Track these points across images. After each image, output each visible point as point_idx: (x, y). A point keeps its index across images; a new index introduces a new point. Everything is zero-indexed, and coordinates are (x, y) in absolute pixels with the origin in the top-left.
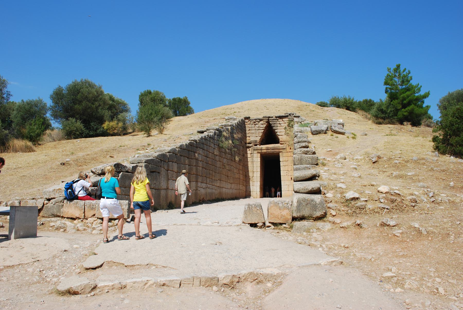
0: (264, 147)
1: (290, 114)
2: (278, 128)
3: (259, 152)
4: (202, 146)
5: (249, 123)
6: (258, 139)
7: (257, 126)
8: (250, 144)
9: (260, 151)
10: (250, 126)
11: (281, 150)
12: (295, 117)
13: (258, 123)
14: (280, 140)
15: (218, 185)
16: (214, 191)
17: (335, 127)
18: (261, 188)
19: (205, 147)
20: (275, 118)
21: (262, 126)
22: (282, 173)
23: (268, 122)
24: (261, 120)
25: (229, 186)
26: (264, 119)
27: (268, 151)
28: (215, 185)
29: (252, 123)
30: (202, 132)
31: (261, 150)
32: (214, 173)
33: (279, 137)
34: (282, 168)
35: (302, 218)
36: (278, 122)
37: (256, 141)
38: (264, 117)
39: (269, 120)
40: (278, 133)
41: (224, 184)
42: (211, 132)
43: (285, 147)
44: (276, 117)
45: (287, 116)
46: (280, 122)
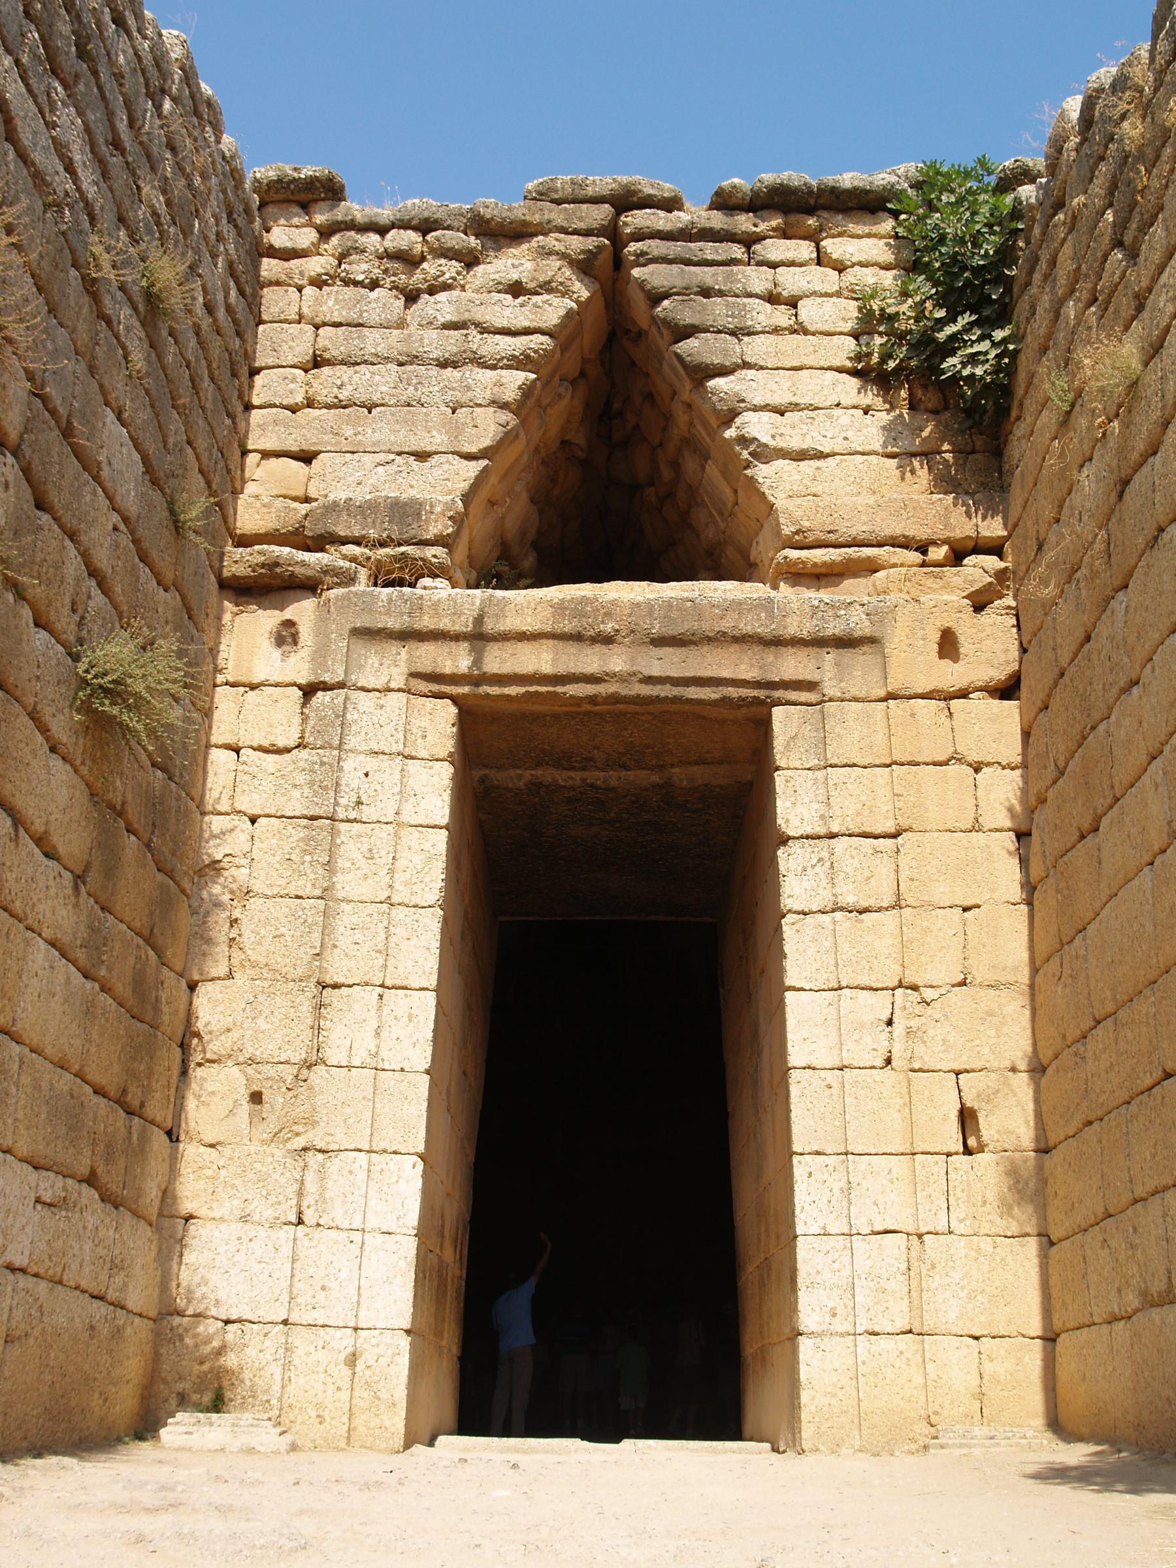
0: (529, 605)
2: (756, 348)
5: (316, 265)
6: (443, 486)
9: (458, 660)
10: (333, 303)
11: (792, 665)
13: (450, 268)
18: (428, 1273)
20: (717, 220)
21: (510, 312)
23: (607, 266)
24: (503, 234)
26: (556, 215)
27: (590, 660)
29: (359, 269)
31: (478, 637)
33: (763, 473)
34: (806, 953)
36: (758, 279)
37: (405, 511)
39: (612, 231)
40: (757, 426)
43: (857, 622)
44: (724, 202)
46: (791, 281)
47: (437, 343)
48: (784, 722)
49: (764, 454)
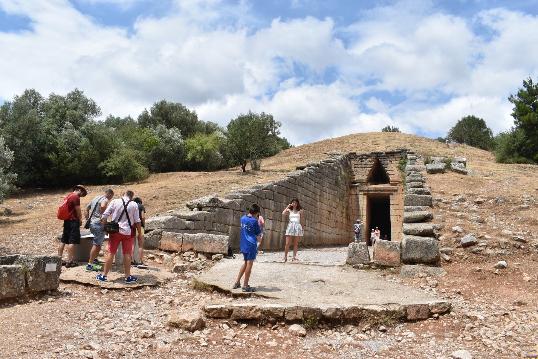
1: (403, 150)
2: (389, 165)
3: (364, 194)
4: (301, 183)
5: (354, 159)
6: (365, 178)
7: (364, 163)
8: (355, 183)
12: (409, 153)
13: (364, 160)
14: (391, 179)
15: (318, 228)
16: (313, 234)
17: (455, 165)
19: (305, 185)
21: (369, 163)
22: (392, 218)
25: (330, 230)
28: (315, 227)
29: (358, 159)
30: (302, 168)
31: (368, 191)
32: (313, 215)
34: (392, 213)
35: (412, 262)
36: (389, 159)
38: (372, 153)
40: (388, 172)
41: (324, 228)
42: (311, 169)
43: (396, 188)
45: (400, 152)
47: (364, 166)
48: (390, 196)
49: (389, 174)
